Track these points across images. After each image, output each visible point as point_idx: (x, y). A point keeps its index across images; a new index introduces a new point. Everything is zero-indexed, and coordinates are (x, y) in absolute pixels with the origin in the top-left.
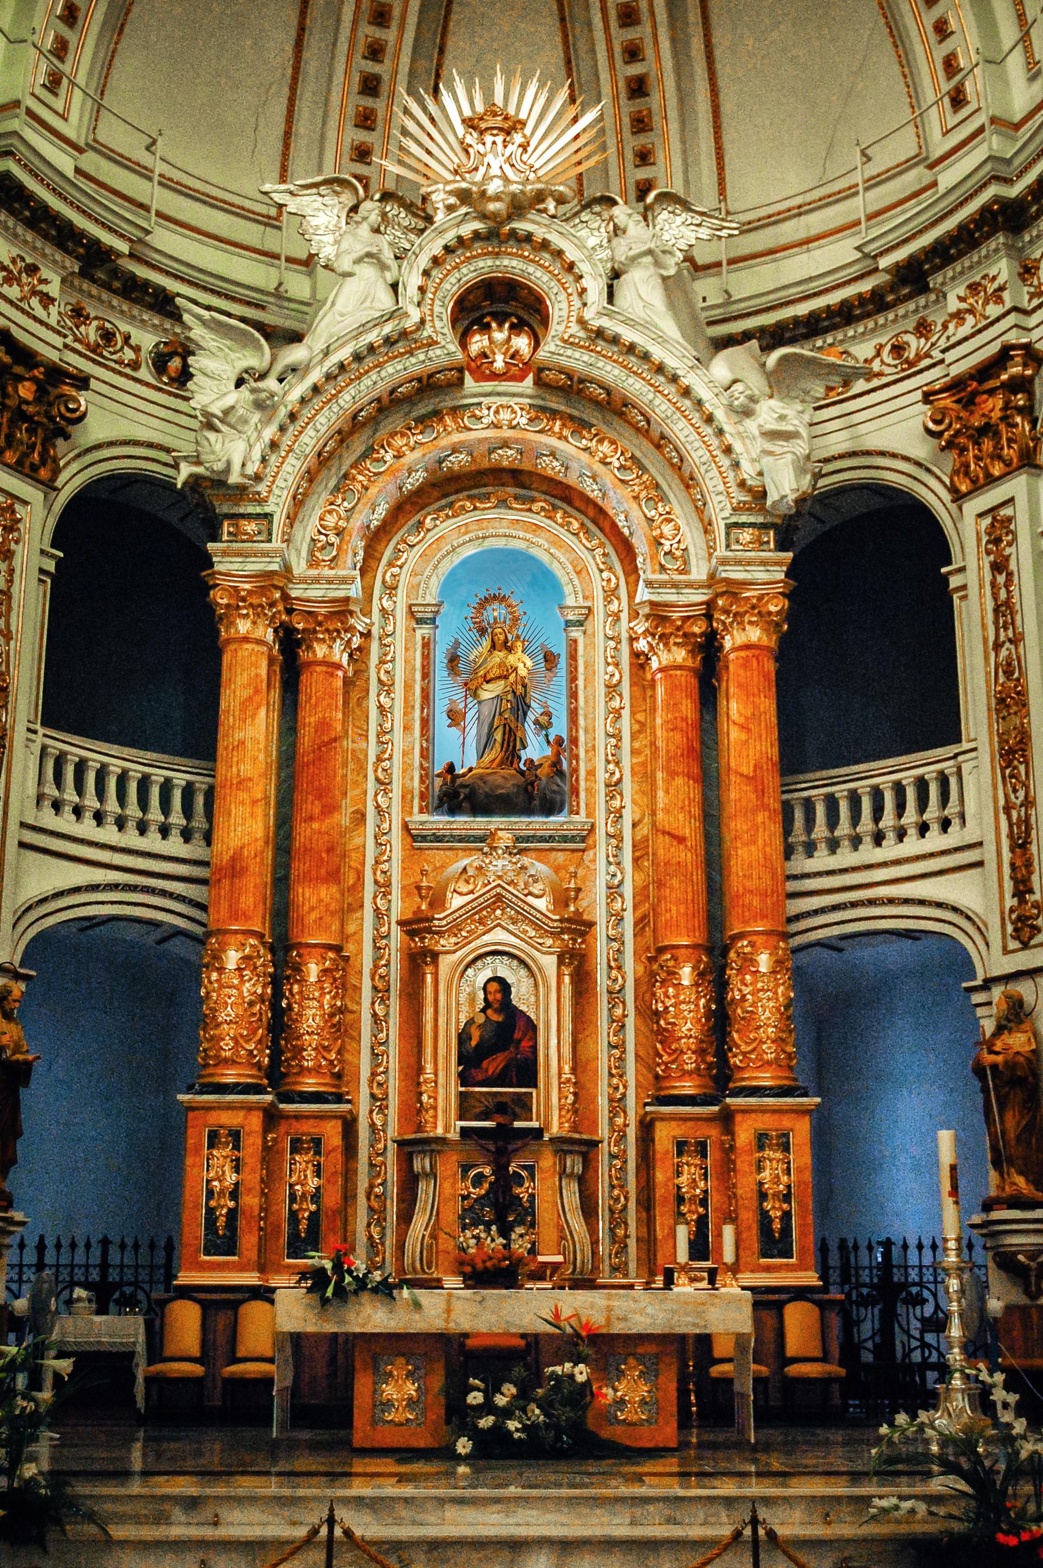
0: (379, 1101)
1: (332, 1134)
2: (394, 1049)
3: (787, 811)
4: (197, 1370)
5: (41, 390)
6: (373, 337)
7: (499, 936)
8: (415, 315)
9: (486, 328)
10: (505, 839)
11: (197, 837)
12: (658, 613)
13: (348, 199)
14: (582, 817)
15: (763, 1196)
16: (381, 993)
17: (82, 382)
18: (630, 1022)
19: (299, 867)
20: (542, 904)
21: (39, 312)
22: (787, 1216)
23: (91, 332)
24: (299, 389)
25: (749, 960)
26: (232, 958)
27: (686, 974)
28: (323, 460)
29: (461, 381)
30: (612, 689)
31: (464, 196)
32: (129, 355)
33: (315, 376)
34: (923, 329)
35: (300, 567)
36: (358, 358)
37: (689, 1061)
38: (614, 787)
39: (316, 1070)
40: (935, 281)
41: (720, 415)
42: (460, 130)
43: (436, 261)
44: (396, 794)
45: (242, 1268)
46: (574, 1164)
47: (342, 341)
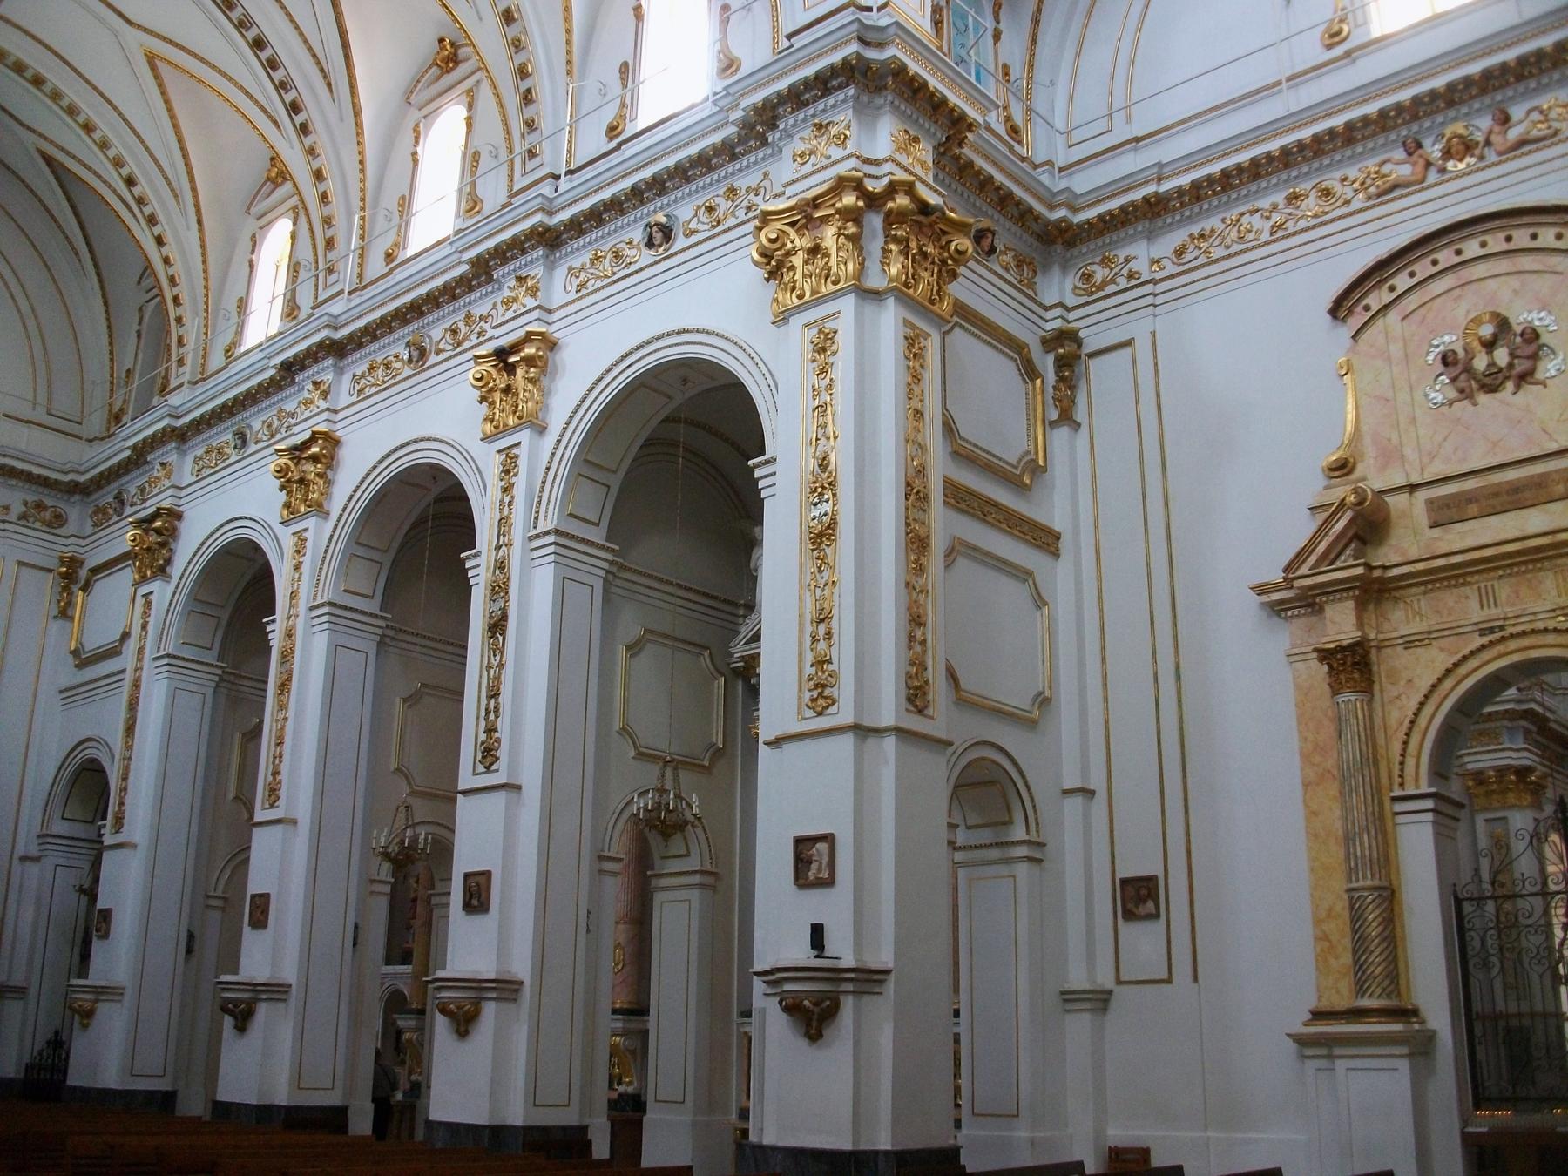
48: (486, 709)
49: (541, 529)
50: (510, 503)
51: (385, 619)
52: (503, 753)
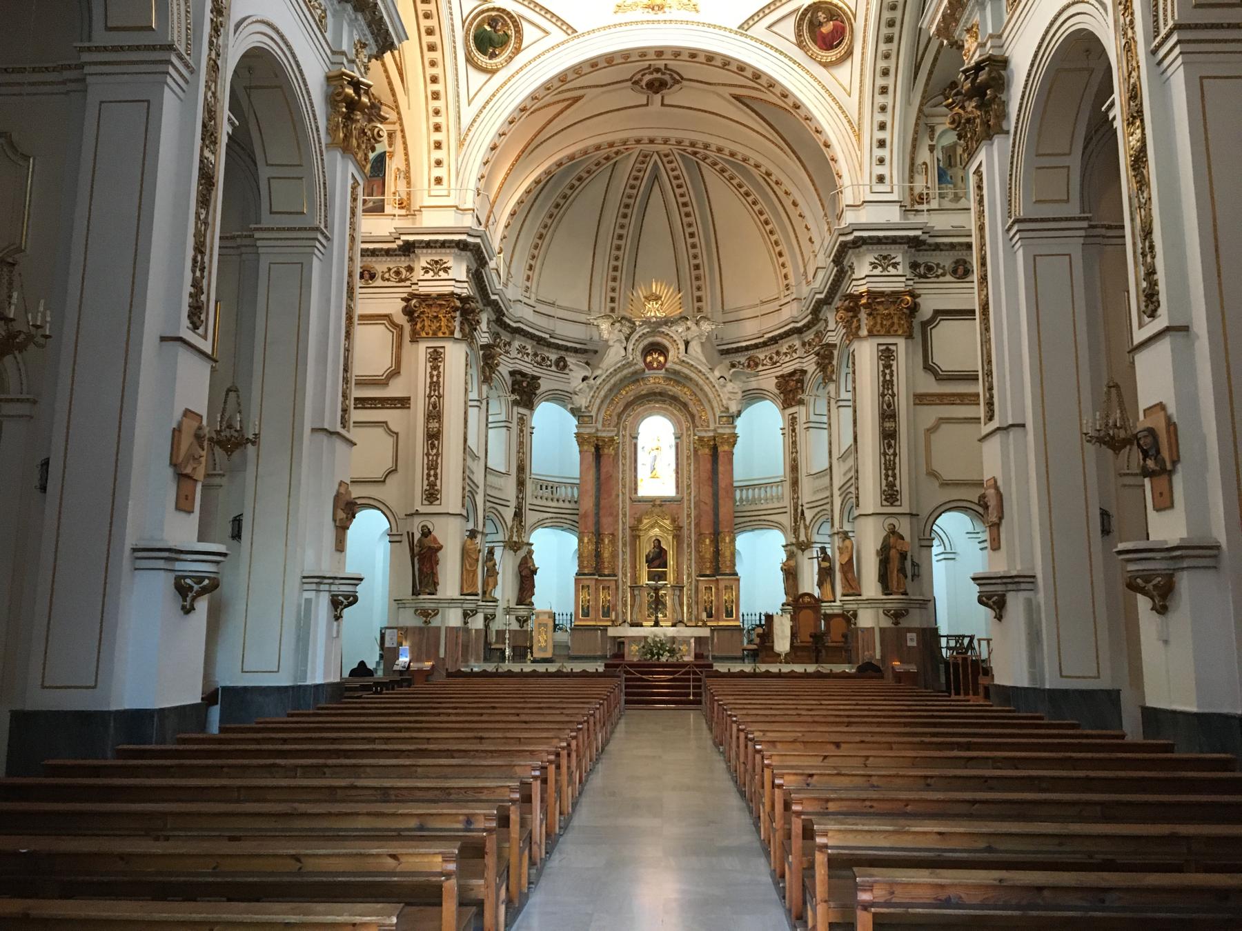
1: (613, 586)
9: (651, 354)
12: (701, 439)
16: (624, 545)
17: (539, 378)
19: (601, 513)
21: (526, 359)
23: (539, 359)
24: (599, 381)
27: (708, 541)
28: (606, 397)
30: (688, 457)
33: (604, 377)
34: (778, 353)
35: (600, 427)
36: (615, 370)
38: (689, 486)
40: (780, 342)
45: (591, 620)
46: (677, 593)
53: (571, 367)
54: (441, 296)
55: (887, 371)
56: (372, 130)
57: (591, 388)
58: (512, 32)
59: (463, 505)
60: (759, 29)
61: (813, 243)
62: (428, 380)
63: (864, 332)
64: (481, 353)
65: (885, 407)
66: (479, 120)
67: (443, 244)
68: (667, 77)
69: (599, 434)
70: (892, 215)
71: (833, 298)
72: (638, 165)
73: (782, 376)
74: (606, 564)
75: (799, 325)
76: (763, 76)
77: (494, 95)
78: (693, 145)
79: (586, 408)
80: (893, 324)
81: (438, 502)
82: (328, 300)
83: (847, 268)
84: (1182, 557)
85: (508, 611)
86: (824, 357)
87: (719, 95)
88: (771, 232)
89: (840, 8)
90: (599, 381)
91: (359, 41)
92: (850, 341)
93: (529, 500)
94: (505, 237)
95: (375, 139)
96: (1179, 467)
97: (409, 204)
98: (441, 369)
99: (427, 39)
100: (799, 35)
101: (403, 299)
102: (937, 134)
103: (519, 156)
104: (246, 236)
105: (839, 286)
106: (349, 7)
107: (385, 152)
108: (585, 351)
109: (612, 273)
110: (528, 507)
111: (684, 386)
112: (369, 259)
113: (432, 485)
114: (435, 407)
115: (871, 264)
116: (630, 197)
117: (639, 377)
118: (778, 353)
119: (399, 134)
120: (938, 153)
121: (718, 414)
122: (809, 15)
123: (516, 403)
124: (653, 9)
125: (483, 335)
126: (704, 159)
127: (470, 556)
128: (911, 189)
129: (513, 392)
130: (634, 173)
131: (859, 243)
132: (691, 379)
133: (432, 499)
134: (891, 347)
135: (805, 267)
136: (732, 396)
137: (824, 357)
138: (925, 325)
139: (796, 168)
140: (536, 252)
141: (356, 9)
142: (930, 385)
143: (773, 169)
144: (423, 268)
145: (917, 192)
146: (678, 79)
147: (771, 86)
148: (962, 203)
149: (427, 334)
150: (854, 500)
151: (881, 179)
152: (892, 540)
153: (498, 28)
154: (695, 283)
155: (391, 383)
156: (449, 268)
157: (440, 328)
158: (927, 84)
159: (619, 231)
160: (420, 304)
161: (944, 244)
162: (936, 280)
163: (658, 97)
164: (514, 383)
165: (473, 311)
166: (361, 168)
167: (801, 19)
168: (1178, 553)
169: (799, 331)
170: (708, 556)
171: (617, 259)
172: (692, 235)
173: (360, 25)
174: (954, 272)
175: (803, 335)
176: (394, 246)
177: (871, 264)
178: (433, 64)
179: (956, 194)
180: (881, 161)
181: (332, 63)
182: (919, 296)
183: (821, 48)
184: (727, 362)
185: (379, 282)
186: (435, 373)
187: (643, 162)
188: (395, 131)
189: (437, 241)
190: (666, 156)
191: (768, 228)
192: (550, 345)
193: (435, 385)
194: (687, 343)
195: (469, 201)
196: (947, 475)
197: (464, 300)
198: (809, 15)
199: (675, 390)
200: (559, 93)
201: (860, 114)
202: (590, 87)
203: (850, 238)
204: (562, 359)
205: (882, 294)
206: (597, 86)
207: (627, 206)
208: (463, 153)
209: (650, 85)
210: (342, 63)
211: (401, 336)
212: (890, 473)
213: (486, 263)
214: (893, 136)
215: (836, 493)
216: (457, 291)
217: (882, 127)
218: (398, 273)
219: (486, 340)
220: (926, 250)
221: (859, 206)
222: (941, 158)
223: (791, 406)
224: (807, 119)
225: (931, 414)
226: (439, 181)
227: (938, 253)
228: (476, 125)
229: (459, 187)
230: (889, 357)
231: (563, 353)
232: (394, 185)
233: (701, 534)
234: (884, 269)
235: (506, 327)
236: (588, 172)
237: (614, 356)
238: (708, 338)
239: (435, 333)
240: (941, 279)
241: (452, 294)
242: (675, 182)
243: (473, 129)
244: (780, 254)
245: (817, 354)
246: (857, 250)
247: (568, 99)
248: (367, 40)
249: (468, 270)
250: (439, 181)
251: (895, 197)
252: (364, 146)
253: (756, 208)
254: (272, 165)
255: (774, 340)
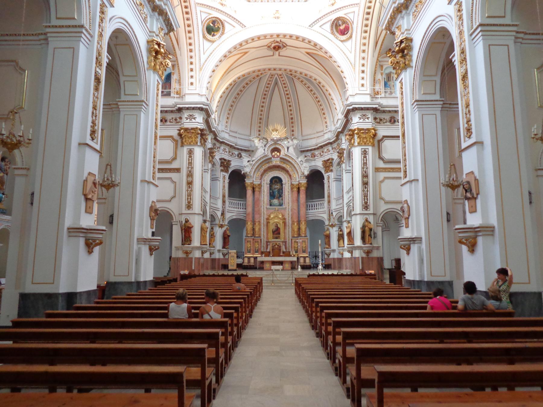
0: (264, 236)
2: (265, 231)
3: (307, 205)
4: (253, 264)
5: (227, 163)
6: (262, 156)
7: (276, 220)
8: (266, 154)
9: (274, 152)
10: (277, 209)
11: (244, 209)
13: (259, 139)
14: (285, 206)
15: (303, 247)
16: (264, 226)
17: (231, 161)
18: (290, 228)
20: (280, 217)
22: (305, 249)
23: (231, 154)
24: (254, 162)
25: (302, 223)
26: (249, 223)
27: (296, 224)
29: (271, 158)
30: (288, 192)
31: (272, 140)
32: (235, 155)
33: (256, 161)
34: (323, 152)
35: (254, 180)
36: (260, 158)
37: (296, 233)
38: (289, 203)
39: (257, 234)
40: (324, 148)
41: (299, 164)
42: (271, 131)
43: (269, 147)
44: (265, 204)
47: (259, 157)
48: (466, 113)
49: (475, 27)
50: (462, 23)
51: (442, 101)
52: (473, 130)
53: (243, 157)
54: (192, 129)
55: (365, 159)
56: (165, 63)
57: (251, 164)
58: (221, 27)
59: (201, 210)
60: (316, 27)
61: (336, 109)
62: (188, 162)
63: (356, 144)
64: (208, 151)
65: (364, 173)
66: (208, 60)
67: (194, 108)
68: (281, 45)
69: (254, 183)
70: (367, 99)
71: (344, 131)
72: (269, 79)
73: (324, 161)
74: (257, 233)
75: (331, 141)
76: (318, 45)
77: (214, 51)
78: (291, 71)
79: (249, 172)
80: (367, 141)
81: (191, 209)
82: (147, 129)
83: (350, 119)
84: (479, 231)
85: (219, 251)
86: (340, 154)
87: (301, 52)
88: (321, 105)
89: (348, 20)
90: (254, 162)
91: (160, 28)
92: (351, 147)
93: (227, 208)
94: (218, 106)
95: (166, 66)
96: (479, 196)
97: (180, 93)
98: (193, 157)
99: (187, 29)
100: (332, 29)
101: (178, 130)
102: (384, 69)
103: (223, 75)
104: (115, 104)
105: (347, 126)
106: (156, 14)
107: (171, 73)
108: (249, 151)
109: (259, 121)
110: (227, 211)
111: (287, 164)
112: (165, 114)
113: (189, 202)
114: (190, 172)
115: (359, 118)
116: (266, 91)
117: (270, 161)
118: (323, 152)
119: (177, 66)
120: (384, 76)
121: (300, 175)
122: (336, 22)
123: (222, 171)
124: (276, 18)
125: (209, 144)
126: (295, 77)
127: (204, 230)
128: (374, 89)
129: (221, 166)
130: (268, 82)
131: (354, 109)
132: (289, 162)
133: (189, 208)
134: (366, 150)
135: (333, 119)
136: (306, 168)
137: (340, 154)
138: (379, 141)
139: (329, 80)
140: (230, 112)
141: (159, 14)
142: (381, 165)
143: (321, 81)
144: (186, 118)
145: (376, 90)
146: (285, 46)
147: (321, 49)
148: (393, 95)
149: (187, 143)
150: (352, 208)
151: (363, 85)
152: (366, 223)
153: (215, 25)
154: (291, 125)
155: (173, 163)
156: (196, 118)
157: (192, 141)
158: (380, 50)
159: (262, 104)
160: (185, 132)
161: (386, 110)
162: (383, 124)
163: (277, 53)
164: (221, 163)
165: (205, 135)
166: (160, 77)
167: (333, 23)
168: (479, 229)
169: (331, 143)
170: (296, 230)
171: (261, 115)
172: (290, 106)
173: (161, 21)
174: (390, 121)
175: (333, 145)
176: (174, 109)
177: (359, 118)
178: (190, 38)
179: (391, 92)
180: (363, 78)
181: (150, 36)
182: (377, 130)
183: (340, 34)
184: (303, 155)
185: (168, 123)
186: (190, 159)
187: (271, 78)
188: (175, 65)
189: (191, 107)
190: (280, 75)
191: (319, 104)
192: (235, 148)
193: (190, 163)
194: (288, 148)
195: (204, 91)
196: (387, 199)
197: (202, 130)
198: (336, 22)
199: (284, 166)
200: (239, 50)
201: (355, 60)
202: (251, 48)
203: (351, 107)
204: (240, 154)
205: (363, 129)
206: (254, 48)
207: (265, 95)
208: (202, 72)
209: (274, 48)
210: (153, 36)
211: (177, 144)
212: (366, 198)
213: (210, 116)
214: (369, 69)
215: (345, 206)
216: (199, 127)
217: (363, 65)
218: (176, 120)
219: (210, 146)
220: (380, 113)
221: (354, 95)
222: (385, 78)
223: (327, 172)
224: (335, 62)
225: (382, 175)
226: (192, 84)
227: (384, 114)
228: (207, 62)
229: (200, 86)
230: (365, 154)
231: (240, 152)
232: (174, 85)
233: (293, 221)
234: (364, 120)
235: (218, 141)
236: (250, 81)
237: (260, 153)
238: (296, 146)
239: (190, 143)
240: (385, 124)
241: (197, 128)
242: (284, 86)
243: (205, 64)
244: (324, 114)
245: (338, 152)
246: (353, 112)
247: (242, 53)
248: (163, 27)
249: (203, 118)
250: (192, 84)
251: (368, 92)
252: (162, 69)
253: (315, 96)
254: (126, 76)
255: (322, 147)
